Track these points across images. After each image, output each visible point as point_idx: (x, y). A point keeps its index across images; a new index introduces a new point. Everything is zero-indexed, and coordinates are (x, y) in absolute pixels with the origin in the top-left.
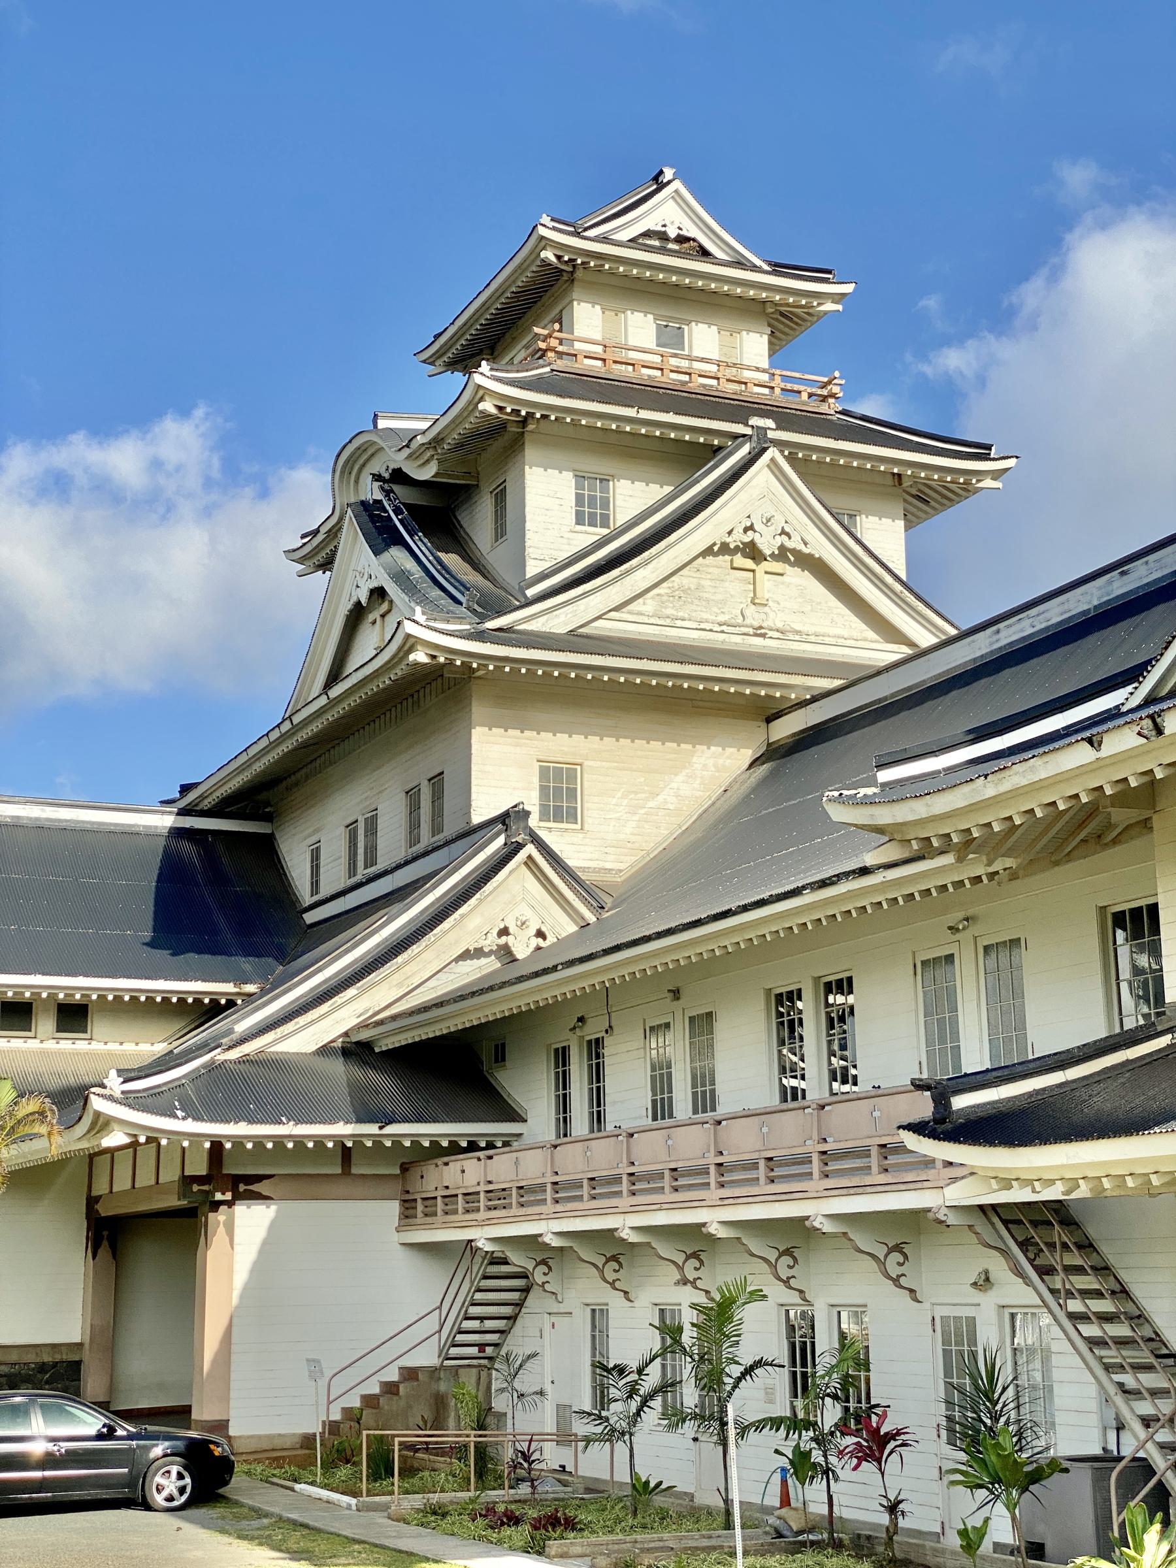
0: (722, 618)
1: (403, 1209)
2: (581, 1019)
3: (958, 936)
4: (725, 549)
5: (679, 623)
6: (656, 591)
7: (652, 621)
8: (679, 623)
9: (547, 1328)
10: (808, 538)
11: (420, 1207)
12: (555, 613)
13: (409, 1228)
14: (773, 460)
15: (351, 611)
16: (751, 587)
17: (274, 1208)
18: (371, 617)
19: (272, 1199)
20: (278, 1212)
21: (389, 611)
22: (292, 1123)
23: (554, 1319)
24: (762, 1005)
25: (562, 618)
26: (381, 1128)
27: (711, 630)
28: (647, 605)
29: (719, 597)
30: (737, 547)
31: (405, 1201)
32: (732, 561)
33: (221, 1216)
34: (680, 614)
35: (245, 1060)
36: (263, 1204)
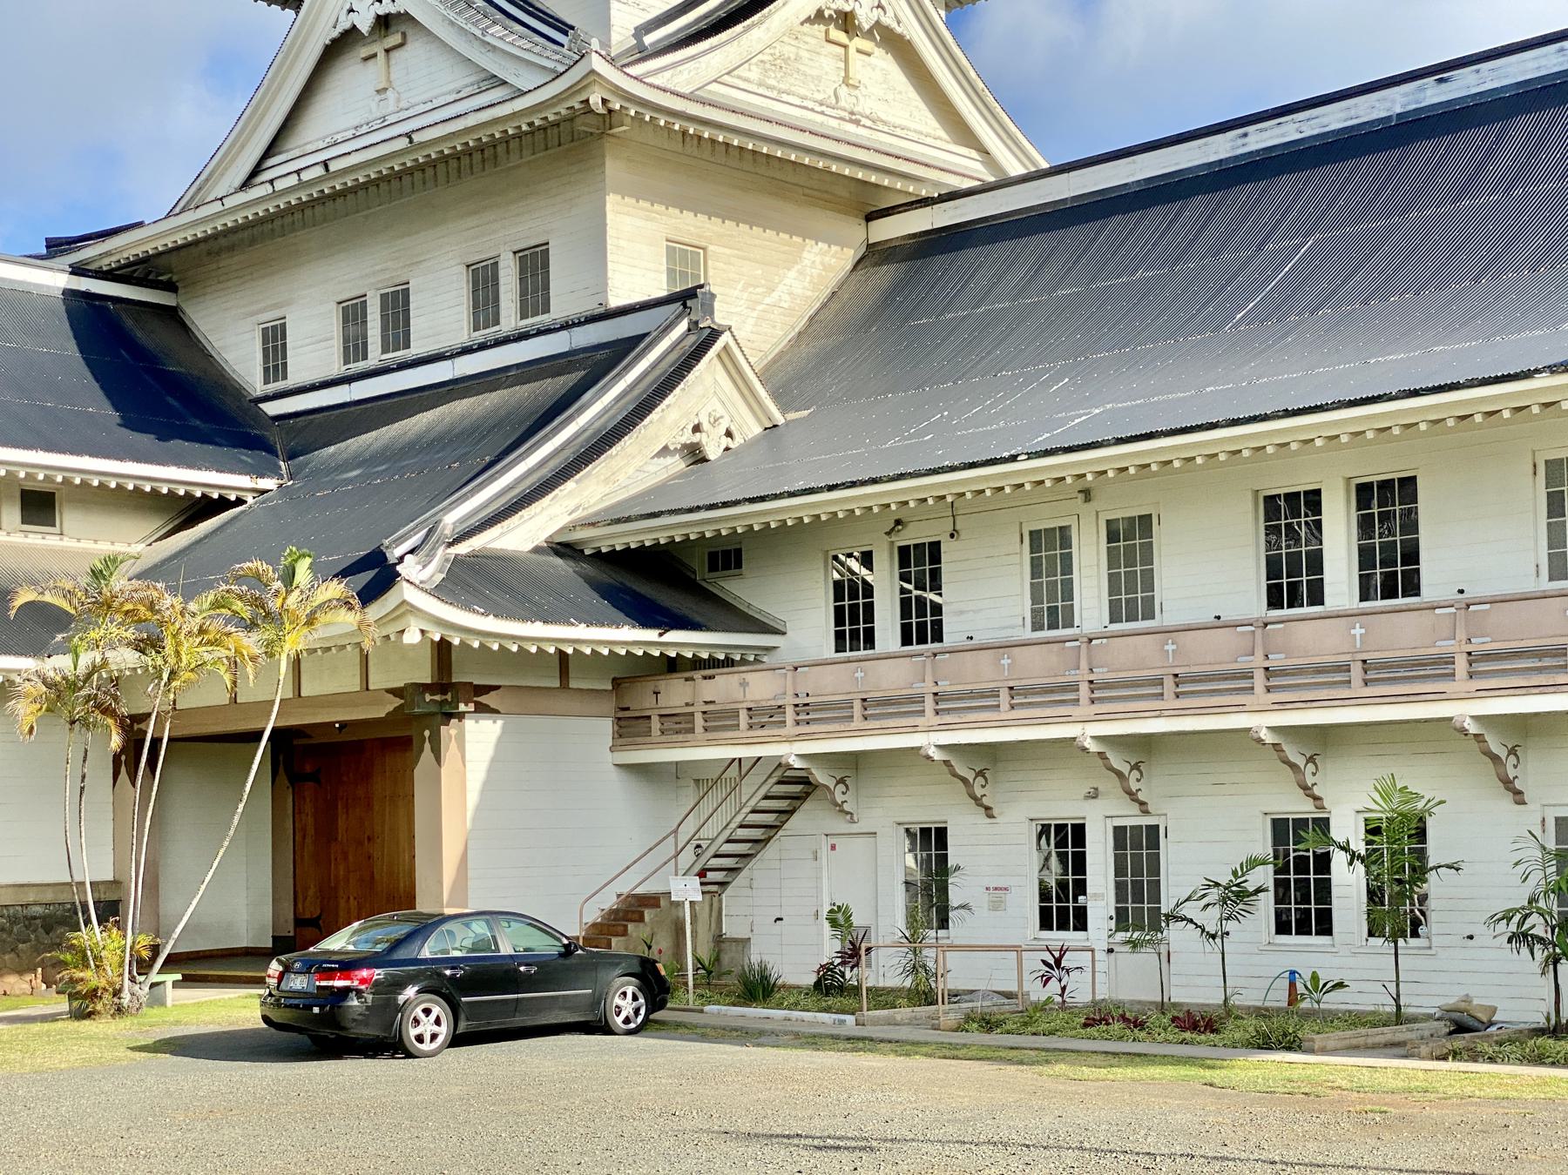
0: (819, 97)
1: (616, 728)
2: (898, 522)
5: (785, 97)
6: (760, 57)
7: (761, 91)
8: (785, 97)
9: (824, 851)
10: (901, 15)
11: (655, 724)
12: (679, 68)
13: (633, 747)
16: (842, 65)
17: (500, 723)
19: (497, 712)
20: (504, 729)
21: (401, 45)
22: (583, 625)
23: (832, 840)
24: (1250, 506)
25: (685, 75)
26: (661, 635)
27: (812, 110)
28: (754, 73)
29: (815, 72)
30: (831, 16)
31: (619, 719)
32: (827, 32)
33: (449, 731)
34: (782, 86)
35: (474, 555)
36: (489, 719)
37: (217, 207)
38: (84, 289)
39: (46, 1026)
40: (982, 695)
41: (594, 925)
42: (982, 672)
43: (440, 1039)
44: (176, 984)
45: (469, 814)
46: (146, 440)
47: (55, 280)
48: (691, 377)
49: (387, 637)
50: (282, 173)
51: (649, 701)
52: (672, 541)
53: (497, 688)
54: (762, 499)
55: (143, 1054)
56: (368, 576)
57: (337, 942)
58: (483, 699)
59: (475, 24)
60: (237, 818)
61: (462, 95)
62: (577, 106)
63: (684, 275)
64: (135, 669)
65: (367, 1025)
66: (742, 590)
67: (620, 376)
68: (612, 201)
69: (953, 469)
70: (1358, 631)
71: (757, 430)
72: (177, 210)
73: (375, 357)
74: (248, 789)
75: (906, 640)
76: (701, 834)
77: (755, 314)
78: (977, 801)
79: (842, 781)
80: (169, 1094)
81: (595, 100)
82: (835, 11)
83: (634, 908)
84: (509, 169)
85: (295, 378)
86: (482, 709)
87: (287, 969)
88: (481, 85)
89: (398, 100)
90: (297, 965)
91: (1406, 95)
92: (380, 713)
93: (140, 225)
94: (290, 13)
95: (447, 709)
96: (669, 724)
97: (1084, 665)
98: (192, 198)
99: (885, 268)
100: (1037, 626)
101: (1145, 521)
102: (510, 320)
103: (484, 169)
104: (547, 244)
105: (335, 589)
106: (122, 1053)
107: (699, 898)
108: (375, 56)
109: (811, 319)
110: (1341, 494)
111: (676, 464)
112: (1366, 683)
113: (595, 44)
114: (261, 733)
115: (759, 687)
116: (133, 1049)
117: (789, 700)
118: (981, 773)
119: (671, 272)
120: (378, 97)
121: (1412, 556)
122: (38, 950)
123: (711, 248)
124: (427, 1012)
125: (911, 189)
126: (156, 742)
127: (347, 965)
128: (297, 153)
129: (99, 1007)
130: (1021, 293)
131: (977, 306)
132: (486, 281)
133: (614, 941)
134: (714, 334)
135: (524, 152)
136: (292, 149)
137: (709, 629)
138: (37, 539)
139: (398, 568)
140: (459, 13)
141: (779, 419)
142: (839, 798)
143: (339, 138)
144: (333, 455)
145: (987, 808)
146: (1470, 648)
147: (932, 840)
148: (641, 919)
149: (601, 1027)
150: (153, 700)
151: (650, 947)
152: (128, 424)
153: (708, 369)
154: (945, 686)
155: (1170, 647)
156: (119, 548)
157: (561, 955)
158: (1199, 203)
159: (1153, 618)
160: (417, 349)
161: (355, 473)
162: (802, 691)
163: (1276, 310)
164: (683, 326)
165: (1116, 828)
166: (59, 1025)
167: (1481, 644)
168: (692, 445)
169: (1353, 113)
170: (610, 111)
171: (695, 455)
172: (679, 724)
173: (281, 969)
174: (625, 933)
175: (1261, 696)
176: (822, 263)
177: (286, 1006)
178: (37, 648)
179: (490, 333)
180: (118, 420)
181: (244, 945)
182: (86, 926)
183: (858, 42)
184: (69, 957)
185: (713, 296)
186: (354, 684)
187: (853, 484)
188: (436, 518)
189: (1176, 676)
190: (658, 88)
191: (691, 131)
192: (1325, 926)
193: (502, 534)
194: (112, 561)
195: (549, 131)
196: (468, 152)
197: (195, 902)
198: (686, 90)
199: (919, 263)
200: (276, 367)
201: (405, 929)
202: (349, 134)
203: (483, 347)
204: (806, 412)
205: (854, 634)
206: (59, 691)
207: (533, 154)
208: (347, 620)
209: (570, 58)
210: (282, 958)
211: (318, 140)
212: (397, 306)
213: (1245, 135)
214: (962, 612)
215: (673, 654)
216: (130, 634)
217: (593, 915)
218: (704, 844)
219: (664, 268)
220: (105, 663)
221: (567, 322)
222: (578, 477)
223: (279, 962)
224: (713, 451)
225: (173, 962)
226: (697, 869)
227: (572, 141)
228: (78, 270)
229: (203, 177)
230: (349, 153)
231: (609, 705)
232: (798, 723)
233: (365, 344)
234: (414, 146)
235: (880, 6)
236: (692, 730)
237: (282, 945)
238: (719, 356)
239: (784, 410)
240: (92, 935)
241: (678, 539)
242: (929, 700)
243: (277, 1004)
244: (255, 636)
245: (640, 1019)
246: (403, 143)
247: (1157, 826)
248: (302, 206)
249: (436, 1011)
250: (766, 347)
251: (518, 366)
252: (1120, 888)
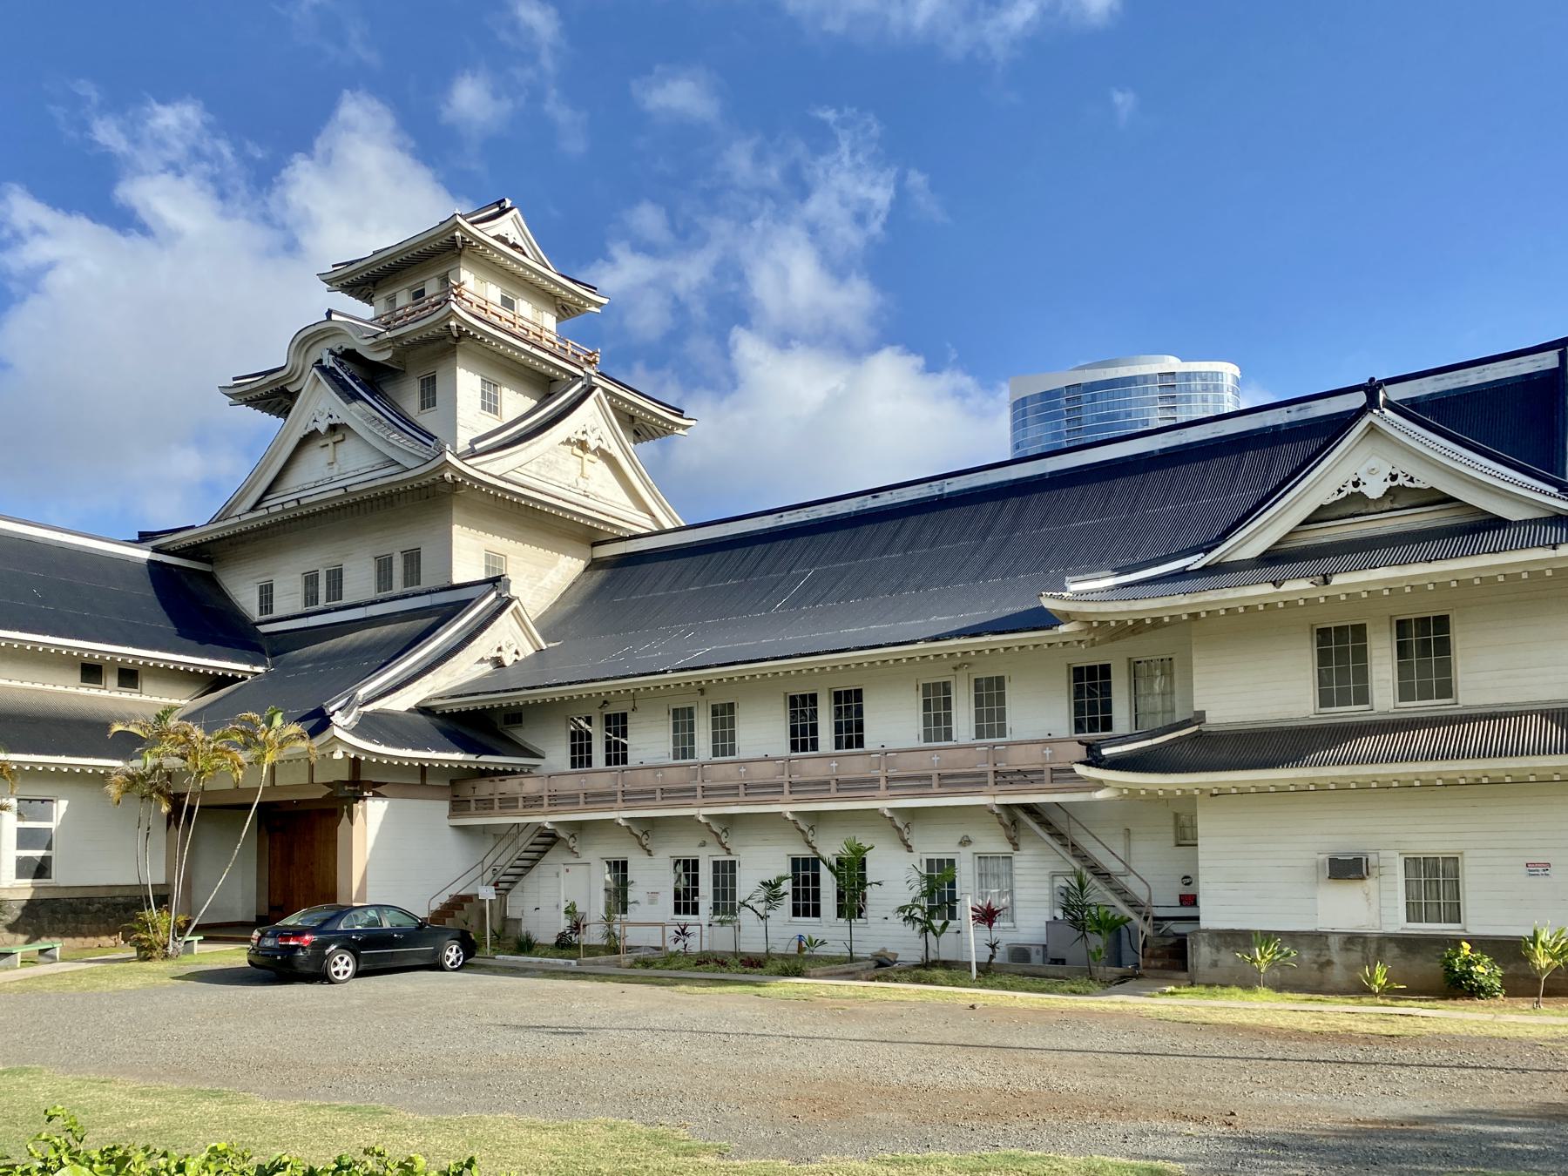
0: (568, 482)
2: (605, 702)
3: (957, 673)
4: (568, 442)
5: (550, 481)
6: (537, 460)
11: (473, 805)
14: (598, 396)
15: (305, 436)
16: (580, 467)
17: (387, 802)
19: (384, 796)
20: (389, 805)
24: (783, 701)
26: (477, 757)
28: (533, 467)
33: (358, 807)
37: (236, 520)
38: (159, 560)
39: (123, 965)
40: (647, 792)
41: (436, 911)
42: (646, 780)
43: (348, 974)
44: (199, 942)
45: (368, 851)
46: (193, 644)
47: (143, 554)
48: (497, 622)
49: (324, 755)
50: (274, 503)
51: (470, 792)
52: (484, 709)
53: (385, 783)
54: (534, 688)
55: (179, 981)
56: (315, 721)
57: (292, 921)
58: (377, 789)
59: (383, 432)
60: (236, 851)
62: (438, 478)
63: (494, 569)
64: (181, 768)
65: (307, 966)
66: (523, 735)
67: (458, 620)
68: (456, 528)
69: (634, 676)
70: (834, 765)
71: (530, 651)
72: (214, 520)
73: (322, 604)
74: (244, 834)
75: (608, 763)
76: (497, 863)
77: (532, 591)
78: (644, 847)
79: (572, 836)
80: (193, 1004)
81: (448, 475)
82: (578, 440)
83: (458, 903)
85: (276, 613)
86: (377, 795)
87: (263, 935)
90: (269, 933)
91: (858, 502)
92: (319, 796)
93: (192, 527)
94: (282, 420)
95: (357, 795)
96: (481, 804)
97: (699, 778)
98: (223, 514)
99: (601, 571)
100: (676, 758)
101: (732, 705)
102: (398, 587)
104: (419, 549)
105: (295, 729)
106: (166, 980)
107: (494, 897)
109: (562, 595)
110: (827, 695)
111: (488, 668)
112: (838, 790)
113: (448, 447)
114: (252, 805)
115: (530, 786)
116: (173, 978)
117: (546, 793)
118: (645, 833)
119: (487, 568)
121: (860, 727)
122: (120, 922)
123: (509, 556)
124: (342, 959)
125: (615, 532)
126: (191, 808)
127: (298, 933)
128: (282, 493)
129: (155, 954)
130: (670, 588)
131: (648, 593)
132: (385, 567)
133: (447, 920)
134: (510, 601)
137: (504, 755)
138: (126, 695)
139: (331, 718)
140: (374, 426)
141: (545, 647)
142: (571, 845)
143: (306, 487)
144: (296, 655)
145: (649, 851)
146: (887, 774)
147: (620, 867)
148: (463, 909)
149: (441, 968)
150: (189, 786)
151: (466, 924)
152: (181, 634)
153: (506, 618)
154: (628, 787)
155: (743, 770)
156: (175, 702)
157: (417, 929)
158: (759, 549)
159: (734, 755)
160: (345, 601)
161: (307, 666)
162: (553, 789)
163: (796, 603)
164: (493, 595)
165: (714, 862)
166: (131, 964)
167: (892, 773)
168: (497, 657)
169: (833, 509)
170: (456, 482)
171: (498, 663)
172: (486, 805)
173: (259, 935)
174: (453, 916)
175: (787, 796)
176: (569, 567)
177: (262, 955)
178: (126, 755)
180: (177, 633)
181: (240, 920)
182: (148, 909)
183: (589, 456)
184: (137, 926)
185: (510, 581)
186: (305, 780)
187: (582, 682)
188: (354, 691)
189: (745, 785)
190: (482, 472)
191: (499, 495)
192: (817, 913)
193: (391, 701)
194: (169, 710)
196: (377, 498)
197: (211, 897)
198: (497, 474)
199: (619, 569)
200: (266, 607)
201: (332, 913)
202: (312, 485)
203: (382, 601)
204: (558, 643)
205: (581, 759)
206: (133, 780)
208: (303, 745)
209: (435, 453)
210: (261, 929)
212: (336, 578)
213: (782, 516)
214: (638, 749)
215: (484, 768)
216: (178, 751)
217: (435, 906)
218: (498, 869)
219: (484, 564)
220: (160, 765)
222: (433, 672)
223: (259, 931)
224: (508, 661)
225: (199, 929)
226: (494, 881)
228: (156, 550)
229: (229, 504)
231: (448, 793)
232: (550, 805)
233: (317, 597)
234: (347, 494)
235: (600, 439)
236: (492, 808)
237: (261, 921)
238: (512, 612)
239: (547, 641)
240: (151, 914)
241: (487, 707)
242: (619, 794)
243: (257, 954)
244: (248, 753)
245: (460, 963)
246: (342, 492)
247: (735, 861)
248: (284, 522)
249: (347, 958)
250: (538, 609)
251: (402, 612)
252: (716, 892)
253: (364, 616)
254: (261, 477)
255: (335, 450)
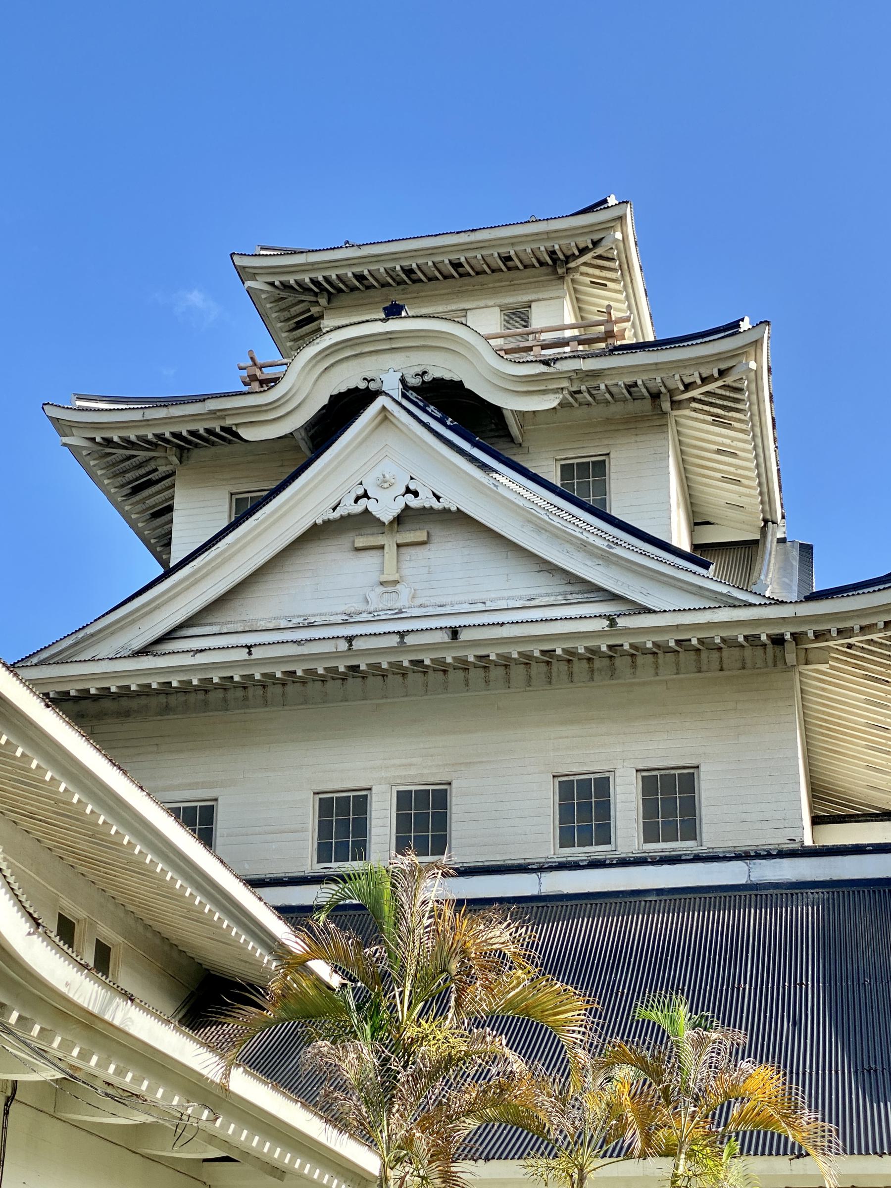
18: (360, 542)
61: (533, 603)
84: (632, 684)
88: (569, 597)
89: (413, 597)
103: (592, 679)
108: (382, 547)
120: (382, 589)
135: (661, 670)
136: (235, 622)
143: (319, 620)
179: (598, 851)
195: (704, 655)
202: (339, 619)
207: (677, 673)
211: (279, 618)
221: (746, 852)
227: (744, 668)
229: (89, 631)
230: (503, 624)
253: (535, 892)
254: (187, 588)
255: (398, 554)
